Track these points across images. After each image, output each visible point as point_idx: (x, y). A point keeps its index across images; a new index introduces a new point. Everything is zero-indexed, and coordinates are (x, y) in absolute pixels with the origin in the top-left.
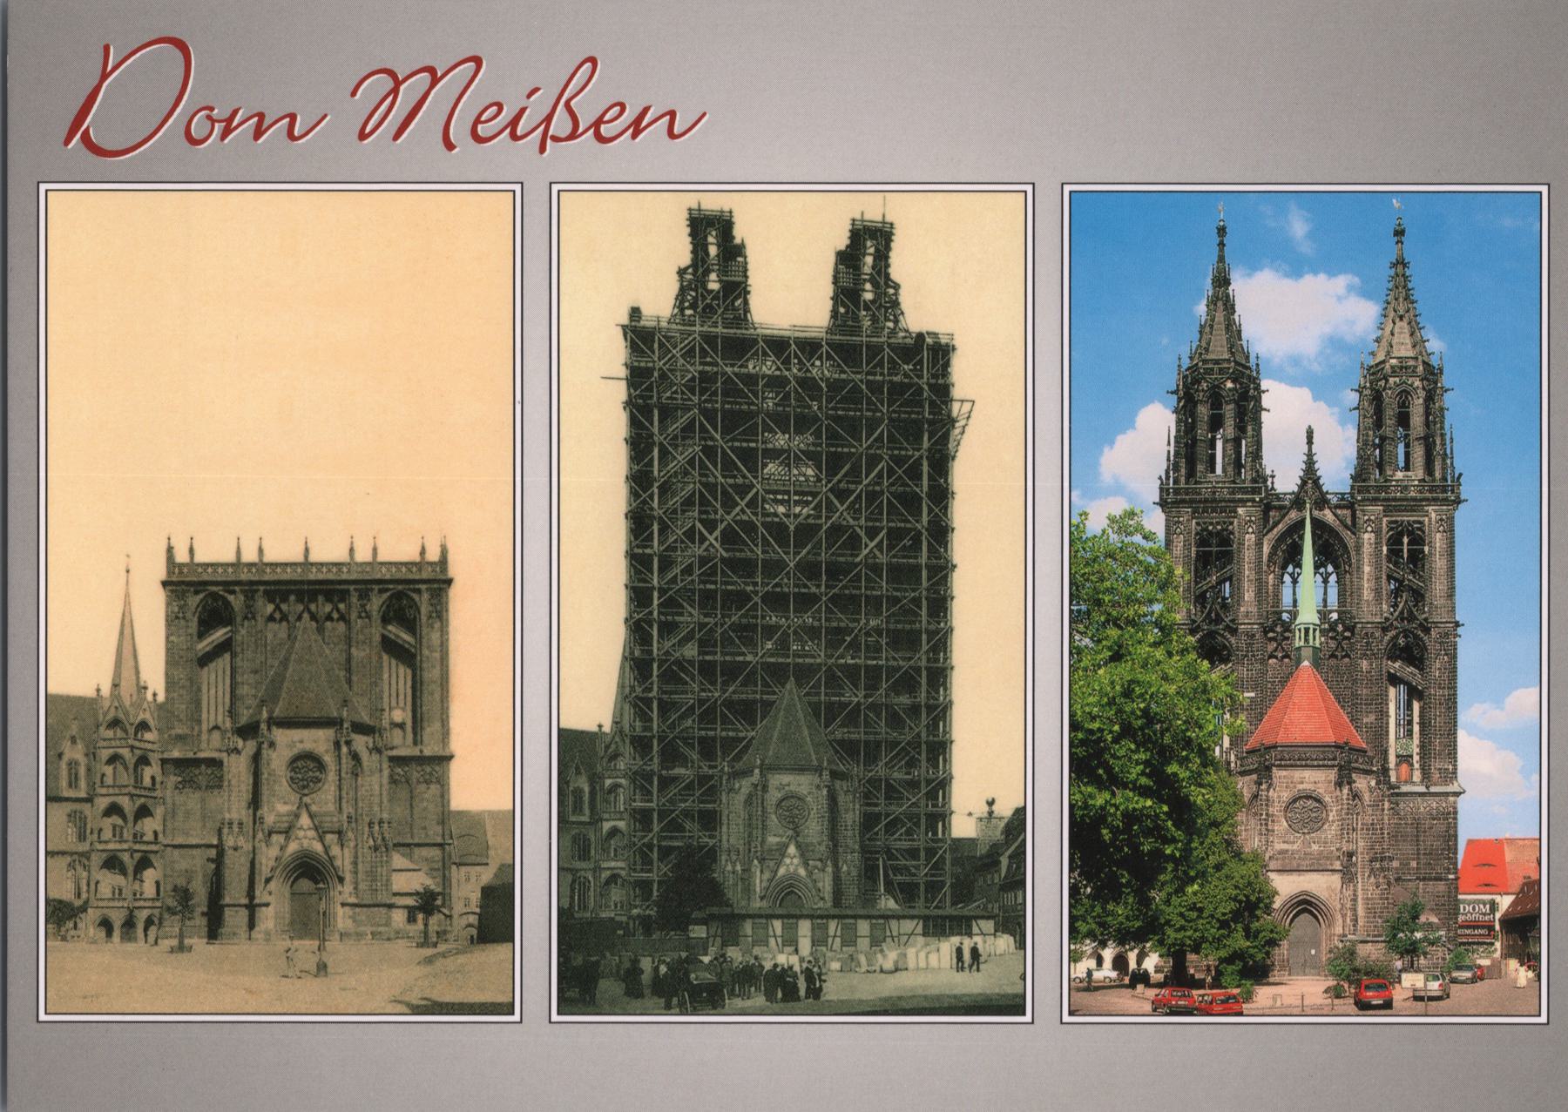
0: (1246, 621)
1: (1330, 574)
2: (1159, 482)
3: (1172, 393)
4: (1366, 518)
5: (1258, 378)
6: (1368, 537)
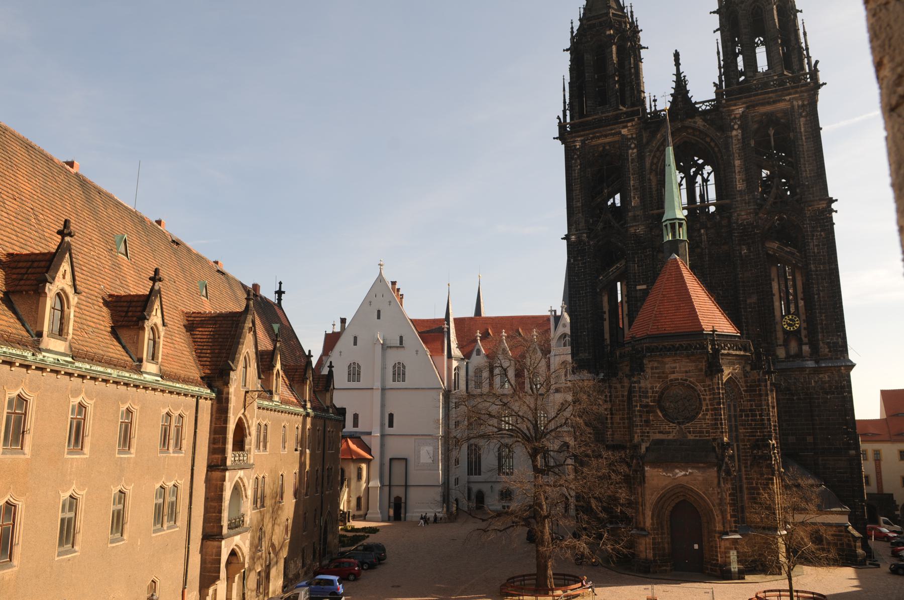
0: (634, 224)
1: (709, 174)
2: (558, 121)
4: (733, 116)
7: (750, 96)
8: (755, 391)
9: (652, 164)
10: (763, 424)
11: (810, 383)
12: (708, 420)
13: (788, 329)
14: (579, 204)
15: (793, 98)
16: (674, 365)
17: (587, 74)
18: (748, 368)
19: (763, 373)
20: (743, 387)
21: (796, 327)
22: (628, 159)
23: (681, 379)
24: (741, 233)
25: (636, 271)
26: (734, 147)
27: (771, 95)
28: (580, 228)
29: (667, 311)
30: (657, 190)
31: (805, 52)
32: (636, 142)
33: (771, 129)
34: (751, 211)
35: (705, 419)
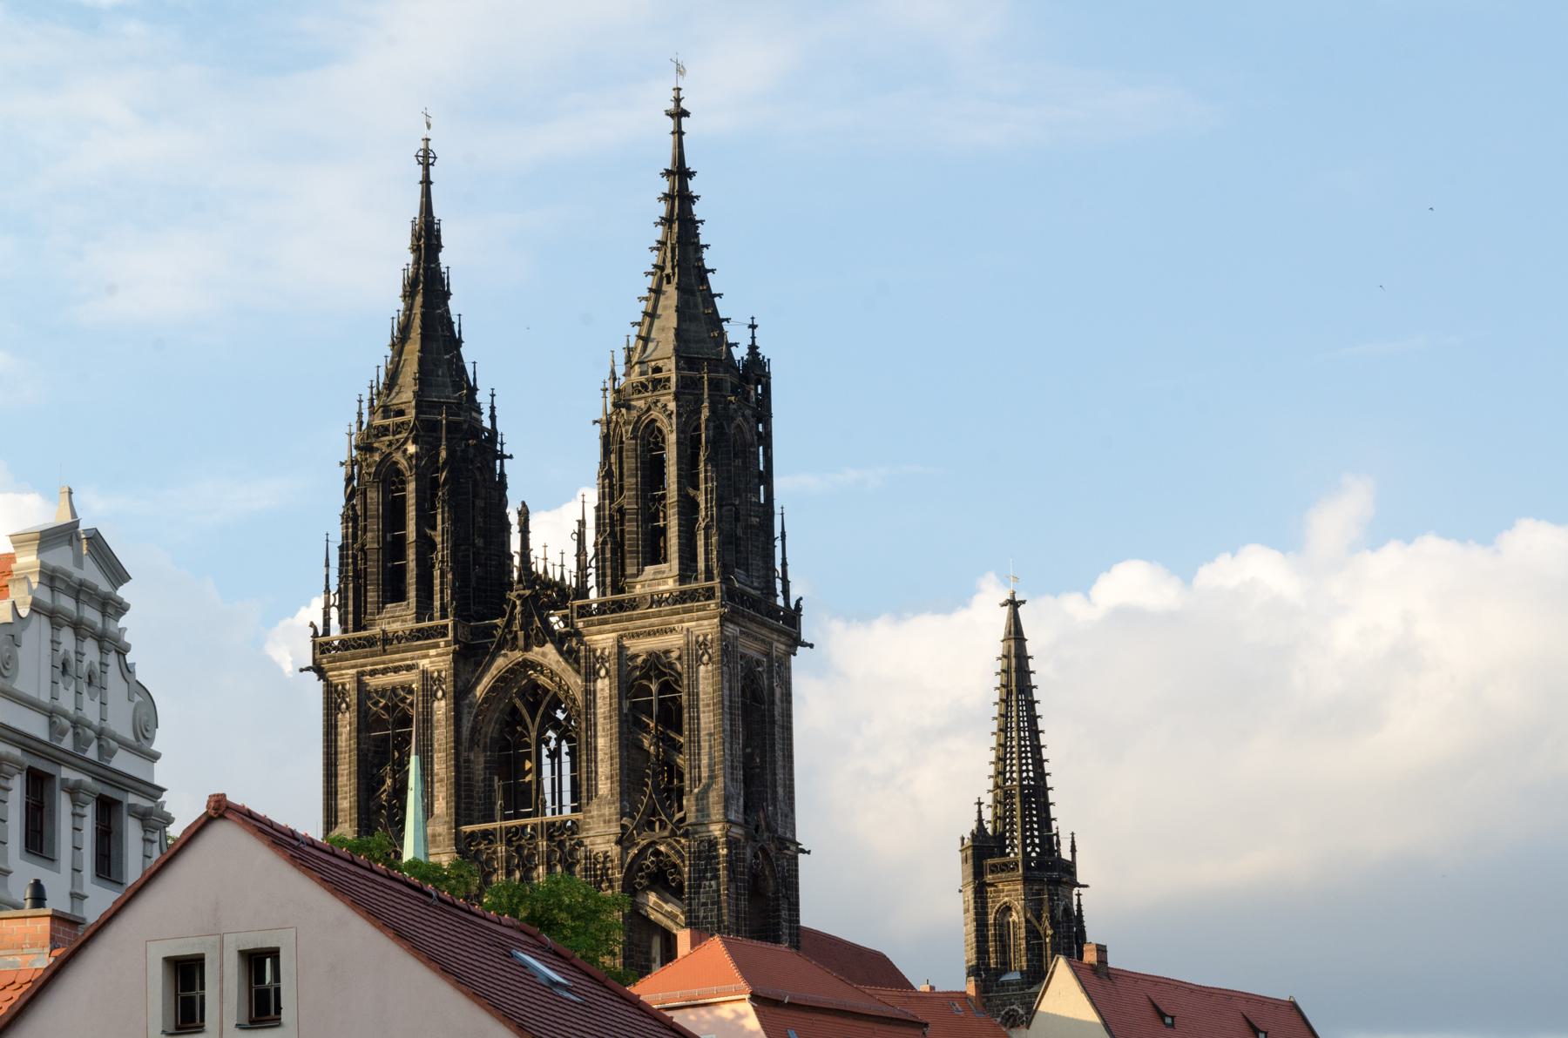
2: (311, 631)
6: (603, 686)
27: (652, 620)
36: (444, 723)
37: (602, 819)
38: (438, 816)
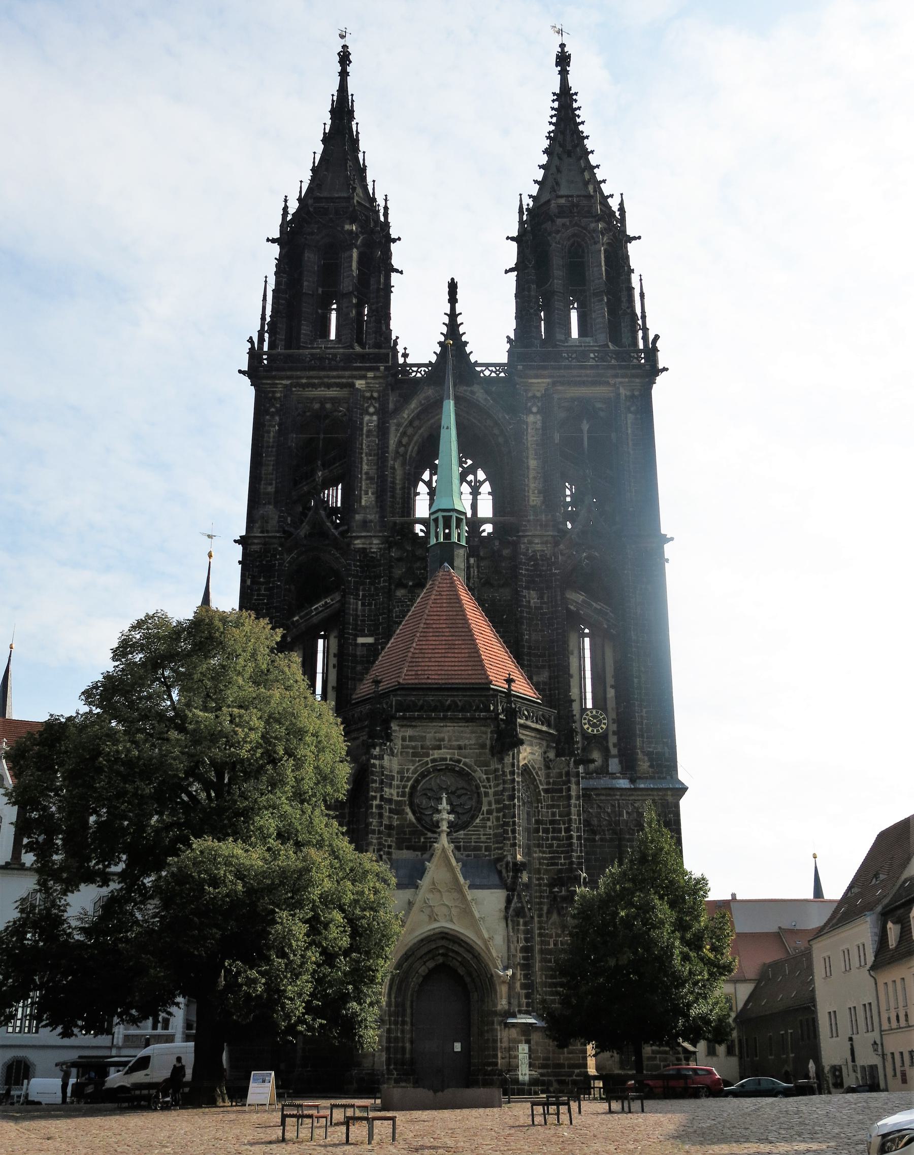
0: (363, 534)
1: (482, 483)
2: (249, 346)
3: (273, 241)
4: (530, 394)
5: (386, 225)
6: (533, 420)
7: (559, 368)
8: (561, 791)
9: (400, 443)
10: (571, 845)
11: (621, 815)
12: (490, 828)
13: (590, 731)
14: (271, 489)
15: (621, 383)
16: (442, 735)
17: (305, 283)
18: (551, 755)
19: (575, 761)
20: (542, 784)
21: (602, 728)
22: (362, 429)
23: (451, 760)
24: (531, 571)
25: (359, 613)
26: (530, 439)
28: (269, 528)
29: (433, 649)
30: (403, 488)
31: (640, 322)
32: (377, 405)
33: (585, 422)
34: (550, 538)
35: (486, 827)
36: (375, 433)
37: (539, 523)
38: (366, 507)
